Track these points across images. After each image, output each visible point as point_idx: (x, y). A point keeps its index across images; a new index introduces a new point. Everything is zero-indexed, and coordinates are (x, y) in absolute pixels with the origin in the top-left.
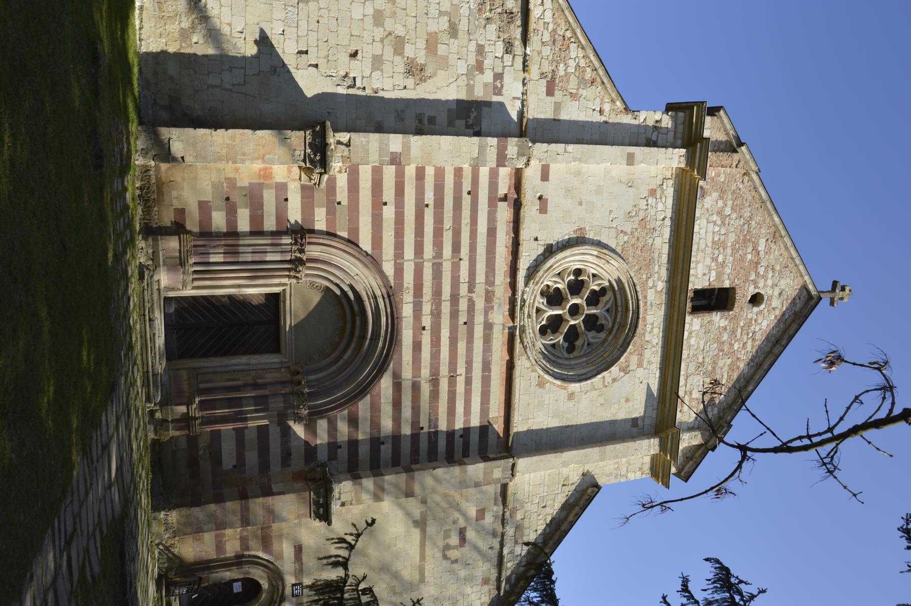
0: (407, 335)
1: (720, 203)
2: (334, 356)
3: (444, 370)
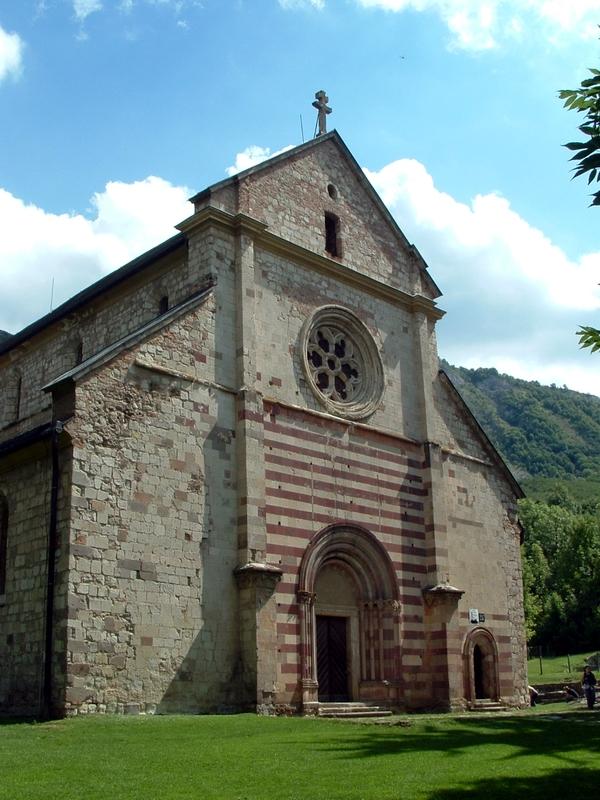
0: (357, 517)
1: (270, 208)
2: (356, 576)
3: (374, 489)
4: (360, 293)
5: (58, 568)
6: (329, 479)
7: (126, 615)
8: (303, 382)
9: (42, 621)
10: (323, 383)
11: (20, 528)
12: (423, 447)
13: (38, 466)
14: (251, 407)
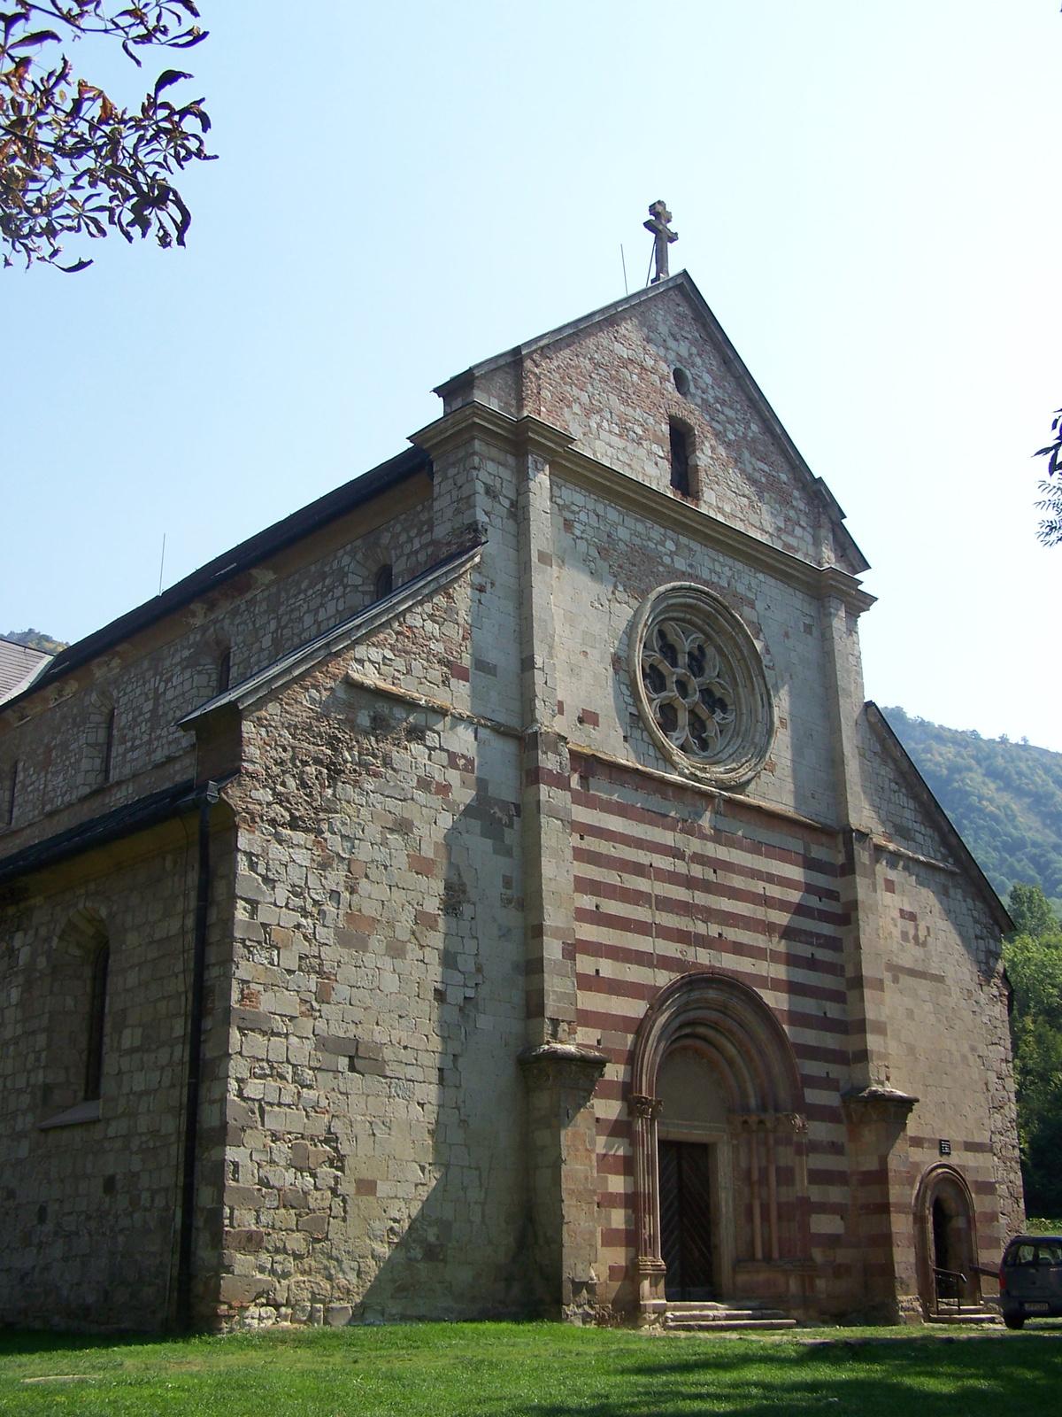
4: (730, 561)
5: (209, 1052)
6: (680, 893)
7: (331, 1138)
8: (637, 719)
9: (176, 1151)
10: (668, 720)
11: (132, 978)
12: (840, 838)
13: (169, 865)
14: (549, 761)
